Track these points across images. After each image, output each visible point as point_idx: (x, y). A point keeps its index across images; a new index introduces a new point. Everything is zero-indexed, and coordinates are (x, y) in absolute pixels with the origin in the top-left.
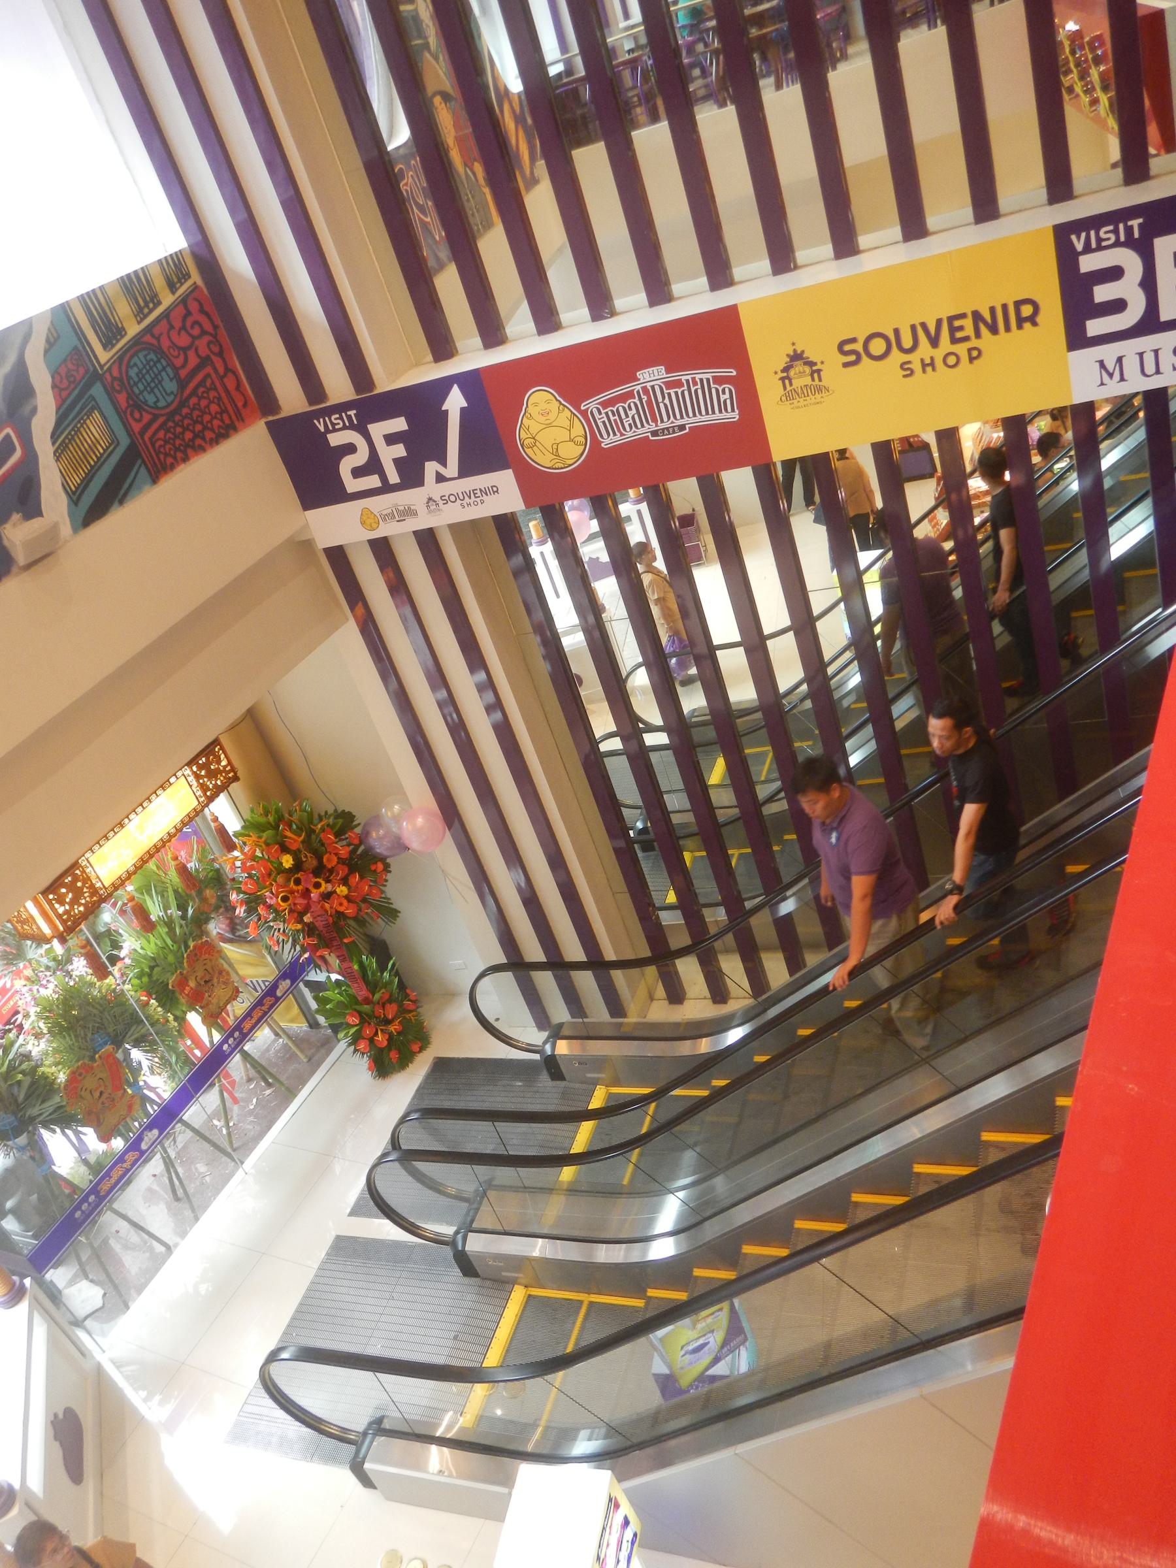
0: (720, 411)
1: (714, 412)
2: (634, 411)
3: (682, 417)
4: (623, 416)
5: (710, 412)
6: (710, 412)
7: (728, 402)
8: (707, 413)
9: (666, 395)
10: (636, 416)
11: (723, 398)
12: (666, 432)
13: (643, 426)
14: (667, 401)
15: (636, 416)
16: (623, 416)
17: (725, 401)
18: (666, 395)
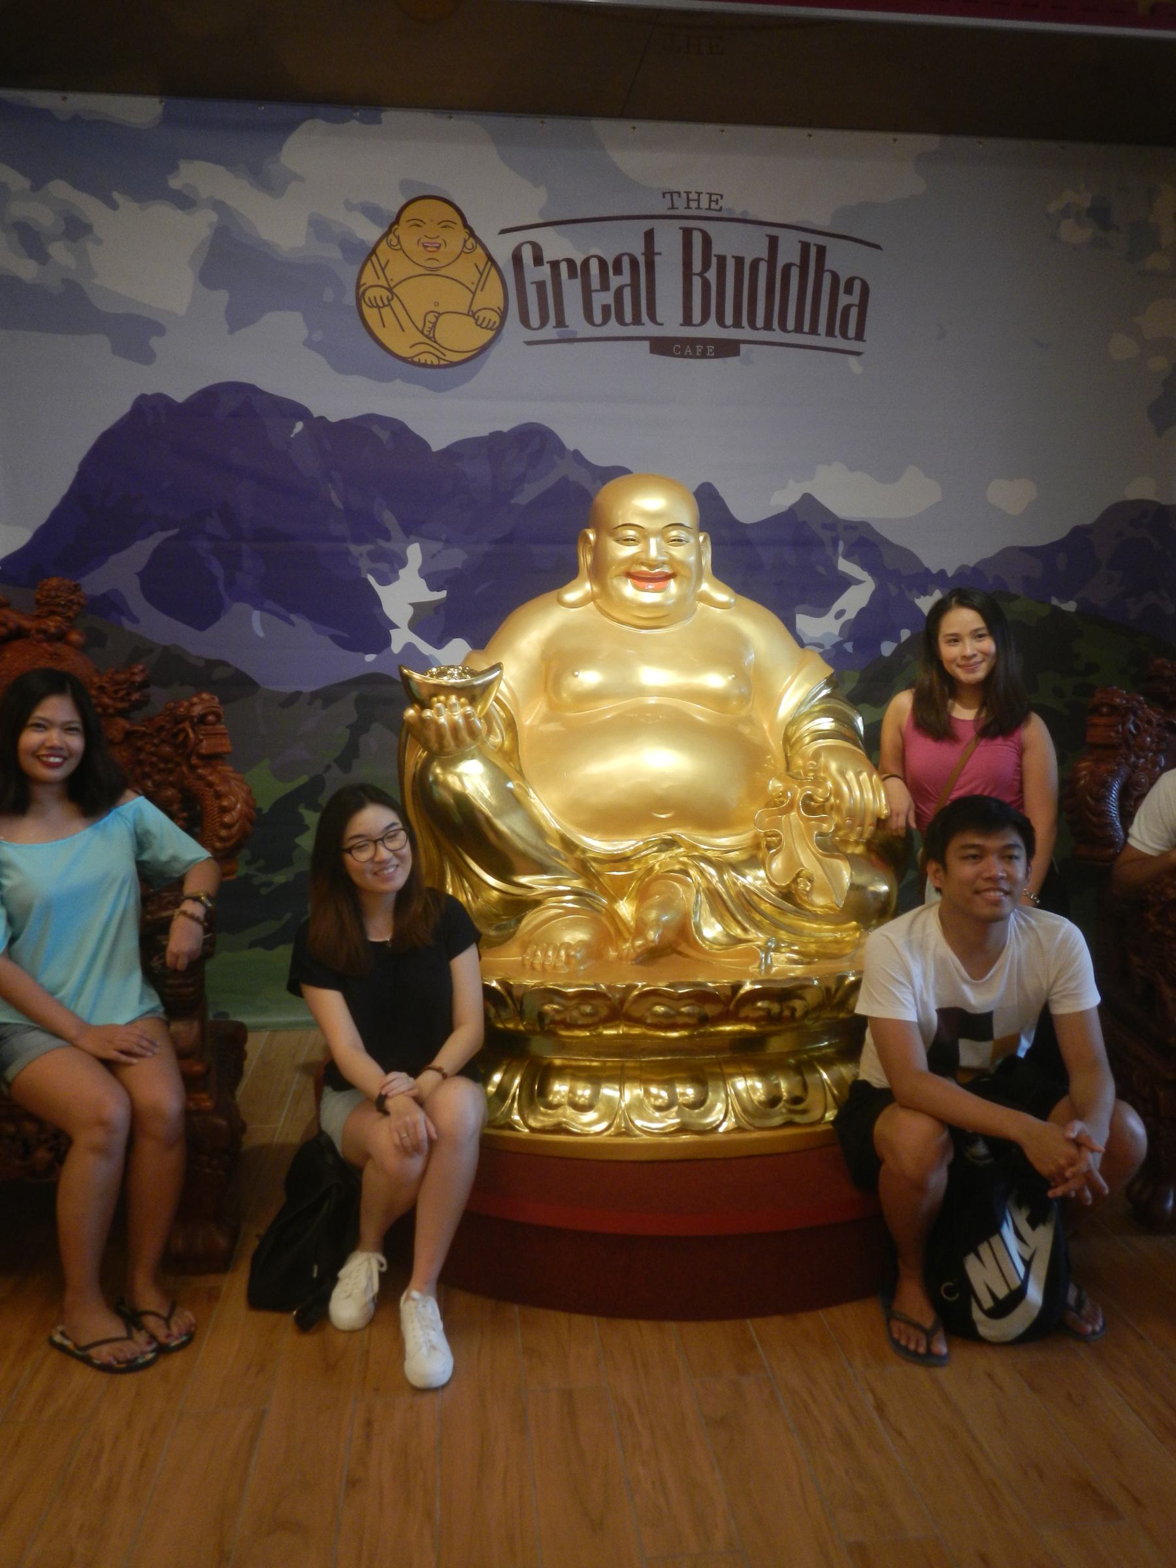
0: (830, 332)
1: (814, 331)
2: (626, 278)
3: (737, 324)
4: (595, 283)
5: (806, 328)
6: (806, 328)
7: (854, 312)
8: (799, 329)
9: (714, 261)
10: (627, 293)
11: (843, 300)
12: (688, 350)
13: (637, 320)
14: (712, 275)
15: (627, 293)
16: (595, 283)
17: (847, 309)
18: (714, 261)
